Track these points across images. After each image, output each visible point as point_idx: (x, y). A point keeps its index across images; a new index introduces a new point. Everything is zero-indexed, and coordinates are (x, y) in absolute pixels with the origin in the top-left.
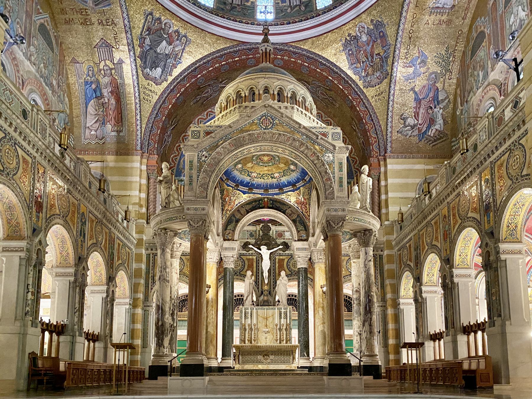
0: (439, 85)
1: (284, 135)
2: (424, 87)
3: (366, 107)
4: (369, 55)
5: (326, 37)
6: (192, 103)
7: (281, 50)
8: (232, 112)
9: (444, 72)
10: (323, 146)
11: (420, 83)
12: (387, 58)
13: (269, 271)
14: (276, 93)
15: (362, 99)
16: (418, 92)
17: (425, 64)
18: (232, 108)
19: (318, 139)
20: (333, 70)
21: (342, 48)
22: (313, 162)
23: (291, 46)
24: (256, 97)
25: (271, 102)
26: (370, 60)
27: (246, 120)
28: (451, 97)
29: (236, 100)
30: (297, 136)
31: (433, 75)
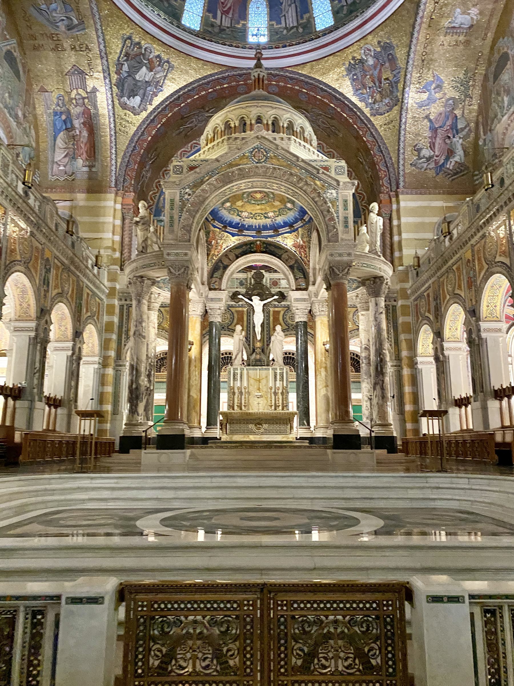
0: (458, 112)
1: (279, 169)
2: (441, 114)
3: (374, 137)
4: (376, 80)
5: (328, 59)
6: (174, 134)
7: (275, 76)
8: (220, 144)
9: (463, 97)
10: (325, 182)
12: (397, 83)
13: (262, 325)
14: (270, 122)
16: (433, 121)
17: (441, 88)
18: (220, 140)
19: (318, 173)
21: (345, 73)
22: (313, 199)
23: (287, 71)
26: (377, 85)
27: (236, 153)
29: (224, 131)
30: (295, 171)
31: (451, 102)
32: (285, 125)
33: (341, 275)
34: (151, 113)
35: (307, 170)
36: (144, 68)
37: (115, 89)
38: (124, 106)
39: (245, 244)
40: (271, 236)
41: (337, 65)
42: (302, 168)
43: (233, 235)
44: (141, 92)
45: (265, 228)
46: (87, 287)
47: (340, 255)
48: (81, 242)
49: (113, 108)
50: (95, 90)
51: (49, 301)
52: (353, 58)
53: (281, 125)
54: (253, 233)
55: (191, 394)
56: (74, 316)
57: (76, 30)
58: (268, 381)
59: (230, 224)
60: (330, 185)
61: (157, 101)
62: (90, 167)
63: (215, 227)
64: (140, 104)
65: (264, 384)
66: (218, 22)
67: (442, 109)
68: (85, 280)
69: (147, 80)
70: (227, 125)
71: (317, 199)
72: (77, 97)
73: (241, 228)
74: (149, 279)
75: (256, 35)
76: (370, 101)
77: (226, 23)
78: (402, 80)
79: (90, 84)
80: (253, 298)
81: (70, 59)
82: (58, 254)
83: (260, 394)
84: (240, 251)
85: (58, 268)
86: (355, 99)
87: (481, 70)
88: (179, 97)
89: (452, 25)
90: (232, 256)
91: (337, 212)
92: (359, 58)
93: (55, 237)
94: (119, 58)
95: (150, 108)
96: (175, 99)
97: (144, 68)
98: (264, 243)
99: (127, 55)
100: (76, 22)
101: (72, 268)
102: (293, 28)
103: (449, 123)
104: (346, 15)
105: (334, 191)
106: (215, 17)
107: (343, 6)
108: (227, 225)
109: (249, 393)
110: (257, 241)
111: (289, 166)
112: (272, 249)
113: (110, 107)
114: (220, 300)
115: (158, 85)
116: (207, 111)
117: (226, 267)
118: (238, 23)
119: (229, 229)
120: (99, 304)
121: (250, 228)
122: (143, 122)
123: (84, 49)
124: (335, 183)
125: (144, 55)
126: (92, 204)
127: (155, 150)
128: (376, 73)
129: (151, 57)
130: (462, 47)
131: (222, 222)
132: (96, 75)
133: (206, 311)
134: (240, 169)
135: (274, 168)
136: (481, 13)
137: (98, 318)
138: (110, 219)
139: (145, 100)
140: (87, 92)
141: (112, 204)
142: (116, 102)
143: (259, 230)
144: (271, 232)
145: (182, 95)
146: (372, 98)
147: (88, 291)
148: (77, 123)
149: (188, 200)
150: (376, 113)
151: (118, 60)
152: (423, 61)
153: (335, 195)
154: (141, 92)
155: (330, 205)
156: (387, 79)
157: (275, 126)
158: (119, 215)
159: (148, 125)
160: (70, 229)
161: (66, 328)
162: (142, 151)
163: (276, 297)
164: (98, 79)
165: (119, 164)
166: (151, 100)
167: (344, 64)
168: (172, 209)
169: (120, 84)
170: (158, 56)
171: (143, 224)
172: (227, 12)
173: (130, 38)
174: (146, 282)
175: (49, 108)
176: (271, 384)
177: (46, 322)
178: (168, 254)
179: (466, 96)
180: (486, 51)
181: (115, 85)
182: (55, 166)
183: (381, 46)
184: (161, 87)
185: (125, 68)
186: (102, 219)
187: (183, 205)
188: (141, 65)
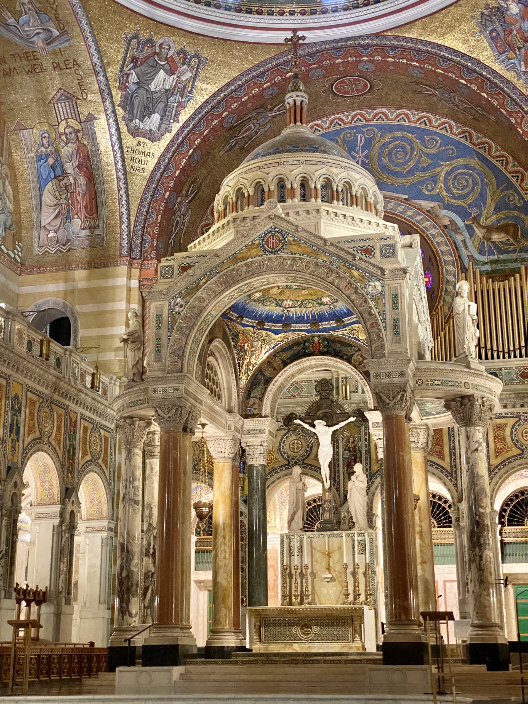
23: (386, 37)
33: (392, 404)
34: (178, 134)
35: (339, 257)
36: (162, 73)
37: (120, 112)
38: (135, 132)
39: (297, 343)
40: (334, 329)
42: (331, 254)
43: (276, 332)
44: (161, 106)
45: (322, 318)
46: (84, 418)
47: (389, 375)
48: (70, 356)
49: (120, 139)
51: (21, 451)
52: (487, 6)
53: (313, 186)
54: (307, 326)
55: (219, 579)
56: (62, 465)
57: (56, 43)
58: (342, 554)
59: (269, 318)
60: (372, 275)
62: (92, 228)
63: (245, 326)
64: (160, 126)
65: (336, 560)
68: (80, 410)
69: (167, 88)
71: (353, 297)
72: (67, 131)
73: (286, 322)
74: (141, 419)
79: (85, 110)
80: (316, 422)
81: (54, 82)
82: (31, 383)
83: (330, 576)
84: (290, 354)
85: (33, 403)
88: (219, 102)
90: (277, 362)
91: (383, 313)
93: (25, 363)
95: (176, 127)
96: (213, 108)
97: (162, 73)
98: (325, 339)
99: (134, 60)
101: (56, 396)
105: (377, 283)
108: (262, 321)
109: (314, 575)
110: (313, 337)
111: (315, 253)
112: (338, 347)
113: (115, 139)
114: (261, 431)
115: (184, 90)
116: (271, 110)
117: (268, 381)
119: (268, 325)
120: (106, 439)
121: (300, 320)
122: (167, 148)
123: (71, 65)
124: (379, 272)
126: (95, 283)
127: (193, 182)
129: (171, 53)
131: (255, 318)
133: (244, 451)
134: (246, 264)
135: (294, 259)
137: (105, 461)
138: (122, 305)
140: (80, 122)
141: (123, 280)
143: (315, 320)
144: (332, 324)
147: (86, 424)
148: (70, 168)
149: (179, 313)
153: (380, 288)
155: (372, 304)
158: (136, 296)
159: (174, 152)
160: (44, 352)
161: (51, 485)
162: (167, 193)
163: (352, 419)
165: (133, 218)
166: (177, 115)
167: (472, 17)
168: (159, 327)
169: (128, 103)
170: (182, 52)
171: (132, 342)
173: (136, 36)
174: (137, 424)
176: (346, 559)
177: (16, 483)
178: (154, 391)
182: (43, 233)
184: (190, 93)
185: (133, 78)
186: (110, 306)
187: (174, 320)
188: (156, 68)
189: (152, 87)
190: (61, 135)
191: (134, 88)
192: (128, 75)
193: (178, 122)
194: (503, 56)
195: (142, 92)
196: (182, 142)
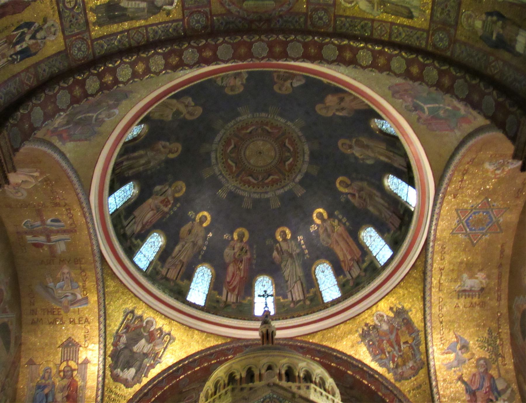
0: (493, 372)
2: (474, 375)
4: (394, 344)
5: (339, 328)
9: (494, 357)
11: (468, 371)
12: (418, 345)
15: (395, 395)
16: (468, 383)
20: (352, 364)
21: (360, 339)
23: (297, 340)
24: (256, 377)
25: (276, 380)
28: (514, 386)
32: (302, 375)
34: (146, 386)
36: (143, 341)
37: (109, 360)
41: (350, 332)
44: (138, 363)
49: (104, 379)
50: (86, 362)
52: (366, 325)
53: (297, 374)
57: (78, 304)
61: (153, 373)
64: (134, 377)
66: (224, 298)
67: (474, 370)
70: (231, 378)
72: (66, 369)
75: (263, 296)
76: (391, 365)
77: (232, 298)
78: (423, 342)
86: (374, 365)
87: (505, 330)
89: (463, 288)
92: (372, 324)
94: (118, 330)
95: (145, 381)
99: (127, 327)
100: (79, 297)
102: (300, 301)
103: (487, 384)
104: (353, 288)
106: (220, 294)
107: (348, 281)
113: (100, 379)
118: (244, 298)
122: (135, 396)
123: (83, 322)
125: (145, 328)
128: (393, 337)
129: (152, 329)
130: (478, 308)
132: (91, 346)
136: (488, 277)
139: (141, 371)
140: (78, 364)
142: (108, 373)
145: (181, 367)
146: (393, 362)
150: (401, 378)
151: (117, 332)
152: (441, 323)
154: (138, 363)
156: (406, 343)
157: (290, 375)
164: (93, 350)
166: (148, 371)
167: (357, 331)
169: (115, 356)
170: (160, 329)
172: (233, 290)
173: (132, 312)
175: (32, 381)
179: (497, 355)
180: (505, 311)
181: (109, 356)
183: (393, 312)
184: (160, 358)
185: (124, 339)
189: (135, 349)
190: (60, 371)
191: (122, 346)
192: (120, 337)
193: (147, 377)
194: (379, 357)
195: (126, 352)
196: (148, 392)
